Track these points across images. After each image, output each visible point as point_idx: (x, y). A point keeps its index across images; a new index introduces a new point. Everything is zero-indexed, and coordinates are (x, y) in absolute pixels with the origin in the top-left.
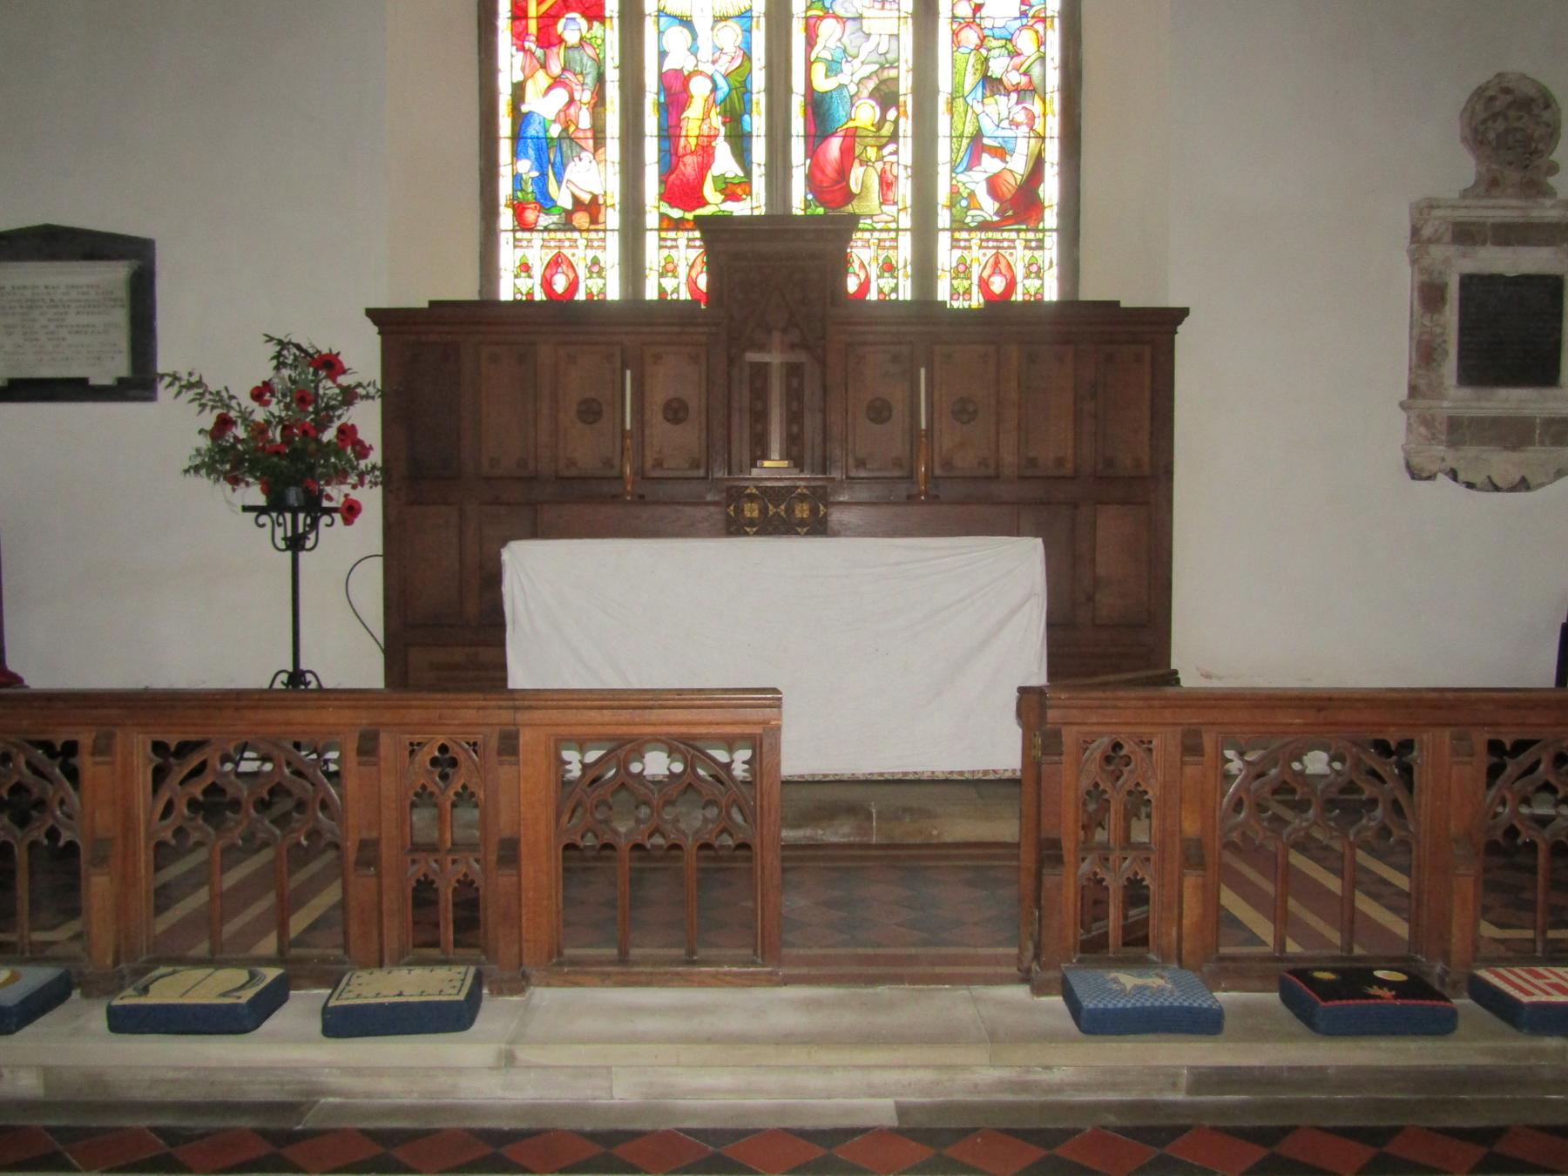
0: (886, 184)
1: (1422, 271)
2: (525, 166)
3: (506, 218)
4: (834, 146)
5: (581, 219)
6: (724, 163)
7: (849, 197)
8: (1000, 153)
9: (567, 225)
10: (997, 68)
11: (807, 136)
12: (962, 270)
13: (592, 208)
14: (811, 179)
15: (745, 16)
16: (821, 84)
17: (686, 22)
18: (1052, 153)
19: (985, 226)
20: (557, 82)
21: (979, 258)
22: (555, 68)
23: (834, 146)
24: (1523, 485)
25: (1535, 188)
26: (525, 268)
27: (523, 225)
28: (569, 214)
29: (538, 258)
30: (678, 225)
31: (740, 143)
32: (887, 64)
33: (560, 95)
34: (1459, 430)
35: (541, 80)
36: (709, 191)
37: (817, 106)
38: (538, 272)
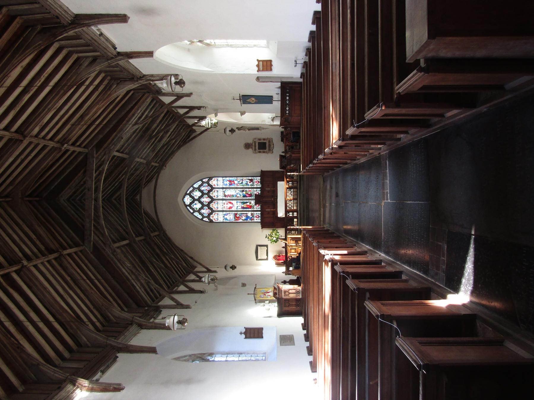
0: (250, 191)
1: (258, 153)
2: (249, 219)
3: (253, 221)
4: (247, 195)
5: (253, 215)
6: (248, 204)
7: (251, 194)
8: (247, 182)
9: (253, 216)
10: (240, 182)
11: (246, 197)
12: (257, 185)
13: (252, 214)
14: (249, 197)
15: (237, 202)
16: (242, 196)
17: (237, 207)
18: (247, 178)
19: (253, 183)
20: (242, 217)
21: (256, 184)
22: (241, 217)
23: (247, 195)
24: (273, 145)
25: (252, 144)
26: (257, 219)
27: (253, 220)
28: (252, 216)
29: (256, 218)
30: (253, 207)
31: (247, 203)
32: (240, 191)
33: (243, 217)
34: (269, 150)
35: (242, 218)
36: (250, 205)
37: (244, 196)
38: (257, 218)
